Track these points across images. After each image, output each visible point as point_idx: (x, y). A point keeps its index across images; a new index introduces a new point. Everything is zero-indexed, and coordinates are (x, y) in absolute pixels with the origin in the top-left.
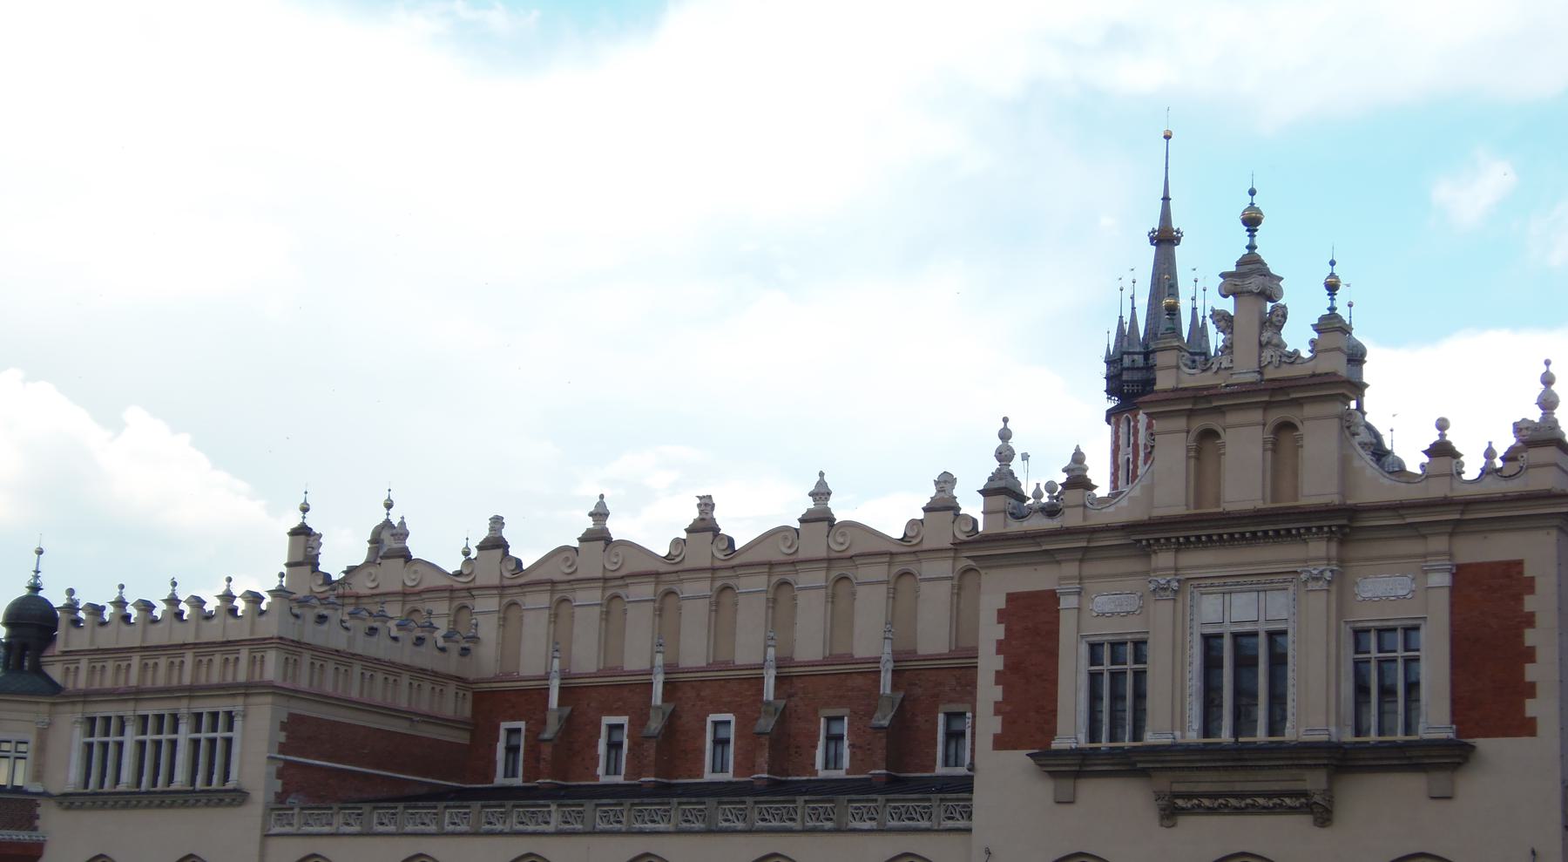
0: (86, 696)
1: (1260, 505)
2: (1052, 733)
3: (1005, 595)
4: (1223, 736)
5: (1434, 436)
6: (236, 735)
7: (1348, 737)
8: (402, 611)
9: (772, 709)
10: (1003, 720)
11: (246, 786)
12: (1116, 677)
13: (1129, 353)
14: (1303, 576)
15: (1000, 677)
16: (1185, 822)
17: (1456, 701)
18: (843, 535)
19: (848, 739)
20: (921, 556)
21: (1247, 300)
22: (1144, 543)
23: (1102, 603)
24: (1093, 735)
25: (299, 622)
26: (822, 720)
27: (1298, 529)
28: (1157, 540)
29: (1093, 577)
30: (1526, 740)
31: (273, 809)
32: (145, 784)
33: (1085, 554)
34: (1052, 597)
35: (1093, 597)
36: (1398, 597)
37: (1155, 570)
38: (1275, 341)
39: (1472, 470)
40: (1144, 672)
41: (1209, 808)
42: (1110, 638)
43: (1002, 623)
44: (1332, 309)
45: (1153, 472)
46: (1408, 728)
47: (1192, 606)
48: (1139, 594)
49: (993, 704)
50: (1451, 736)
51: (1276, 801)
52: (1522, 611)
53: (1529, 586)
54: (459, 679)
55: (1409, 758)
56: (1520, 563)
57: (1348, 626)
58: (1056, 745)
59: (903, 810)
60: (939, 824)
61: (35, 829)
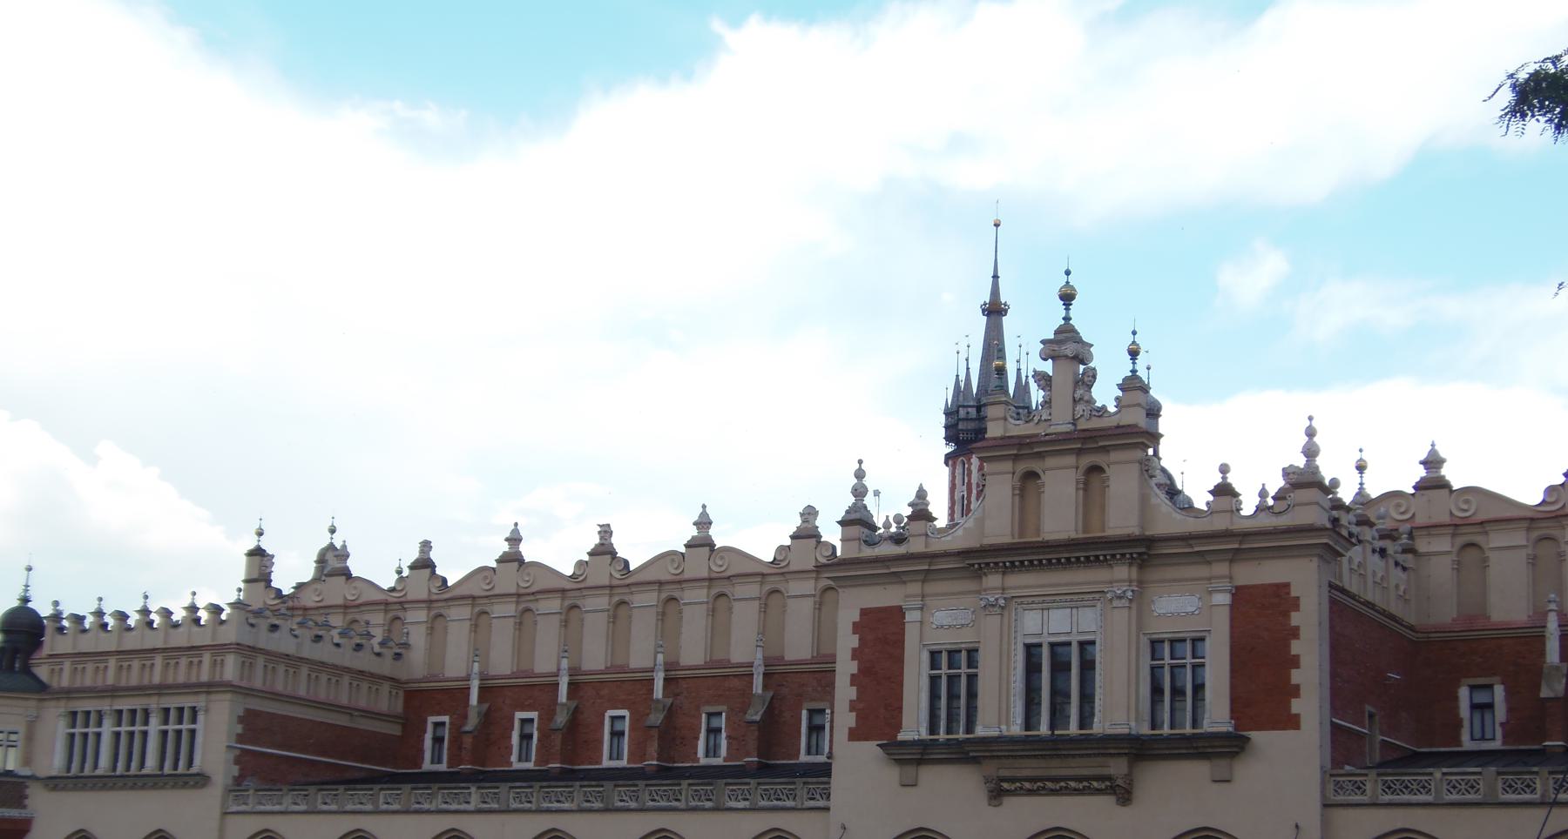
0: (68, 693)
1: (1073, 535)
2: (898, 727)
5: (1218, 479)
6: (199, 726)
7: (1145, 730)
8: (428, 616)
9: (661, 706)
10: (857, 716)
11: (208, 770)
12: (953, 680)
13: (964, 406)
14: (1109, 596)
15: (854, 680)
16: (1010, 803)
17: (1234, 700)
18: (722, 558)
20: (788, 576)
21: (1062, 363)
22: (976, 566)
23: (941, 617)
24: (933, 729)
25: (254, 630)
26: (704, 715)
27: (1105, 556)
28: (987, 564)
30: (1291, 733)
31: (230, 791)
32: (120, 769)
33: (927, 576)
34: (899, 612)
37: (985, 590)
38: (1086, 398)
41: (1029, 790)
44: (1134, 371)
45: (984, 506)
46: (1195, 724)
48: (972, 609)
50: (1231, 729)
51: (1086, 784)
53: (1295, 604)
54: (392, 679)
55: (1197, 748)
58: (901, 737)
59: (772, 792)
60: (802, 804)
61: (25, 807)
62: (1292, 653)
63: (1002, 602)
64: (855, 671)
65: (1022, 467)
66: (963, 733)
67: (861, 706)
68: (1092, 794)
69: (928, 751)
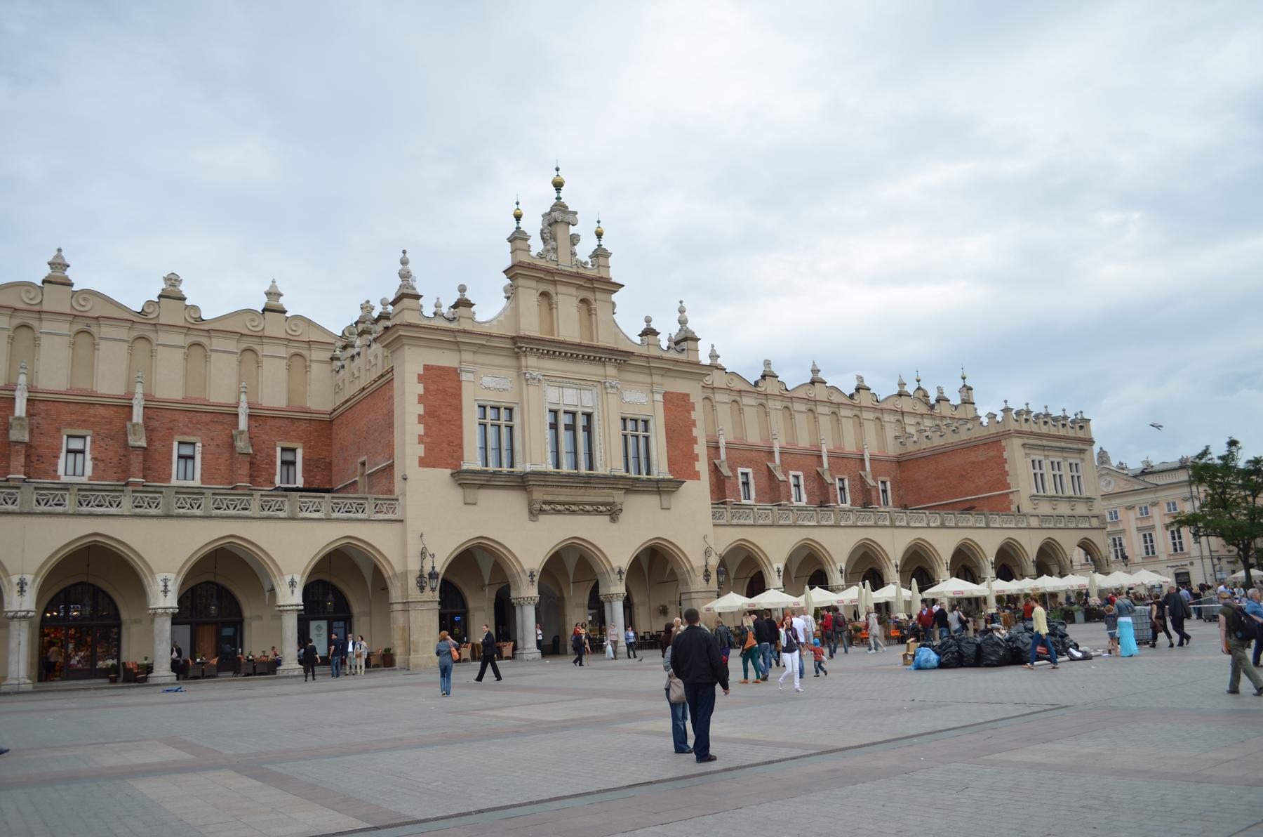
2: (461, 458)
4: (564, 468)
5: (644, 326)
10: (425, 447)
15: (421, 419)
16: (542, 517)
17: (669, 459)
23: (488, 381)
28: (532, 349)
29: (482, 364)
49: (417, 436)
50: (672, 477)
51: (595, 507)
53: (693, 407)
56: (688, 395)
58: (465, 467)
62: (694, 435)
64: (422, 413)
66: (507, 467)
67: (428, 440)
69: (493, 479)
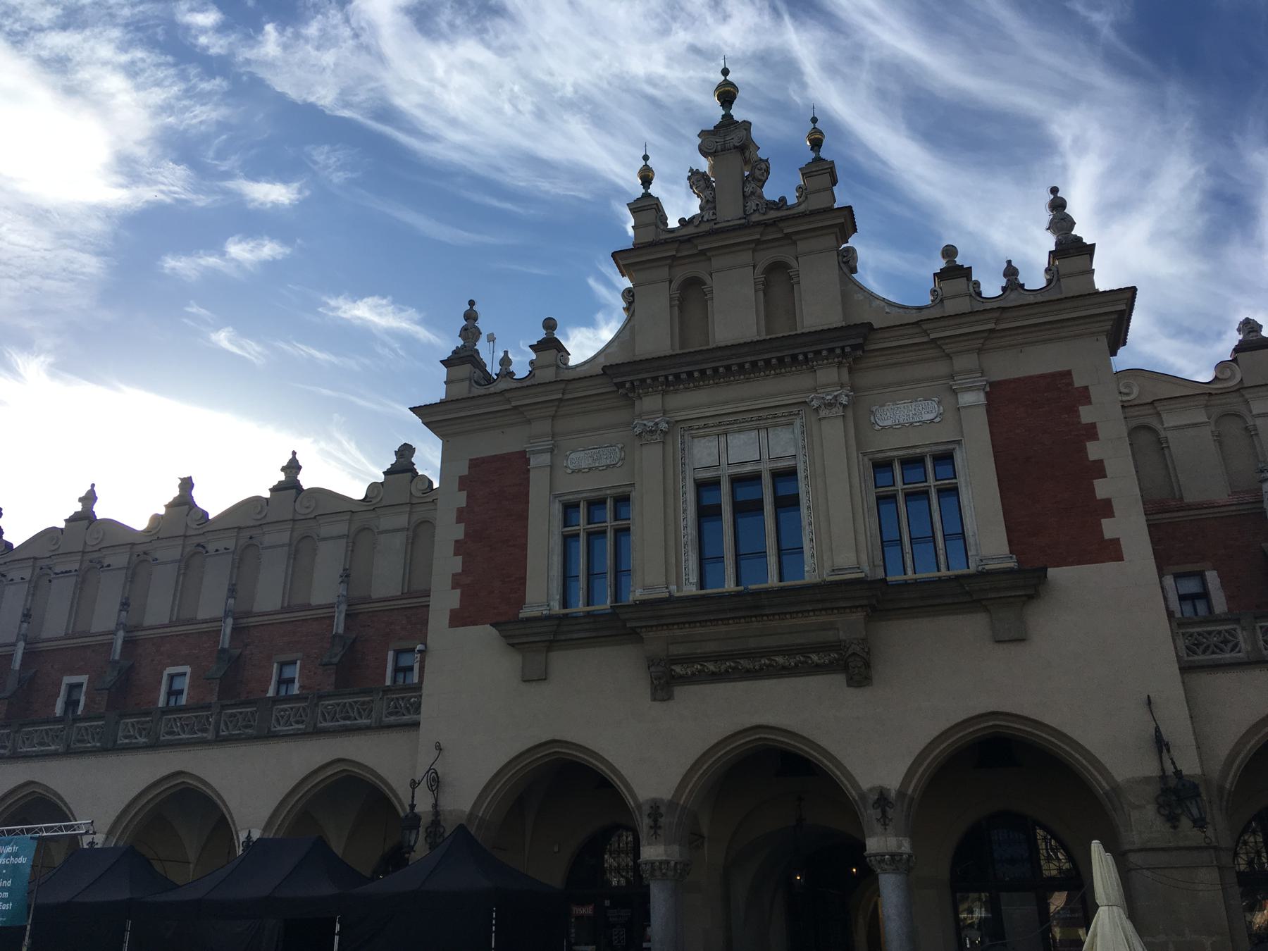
2: (521, 602)
3: (467, 462)
15: (459, 547)
16: (680, 692)
19: (299, 682)
23: (579, 459)
26: (275, 665)
28: (643, 381)
34: (522, 458)
35: (568, 453)
36: (924, 422)
39: (992, 287)
40: (627, 530)
41: (713, 673)
42: (584, 495)
43: (464, 490)
47: (683, 450)
48: (620, 446)
52: (1079, 423)
53: (1084, 396)
56: (1068, 374)
57: (866, 459)
58: (525, 613)
63: (664, 426)
65: (682, 273)
68: (808, 674)
